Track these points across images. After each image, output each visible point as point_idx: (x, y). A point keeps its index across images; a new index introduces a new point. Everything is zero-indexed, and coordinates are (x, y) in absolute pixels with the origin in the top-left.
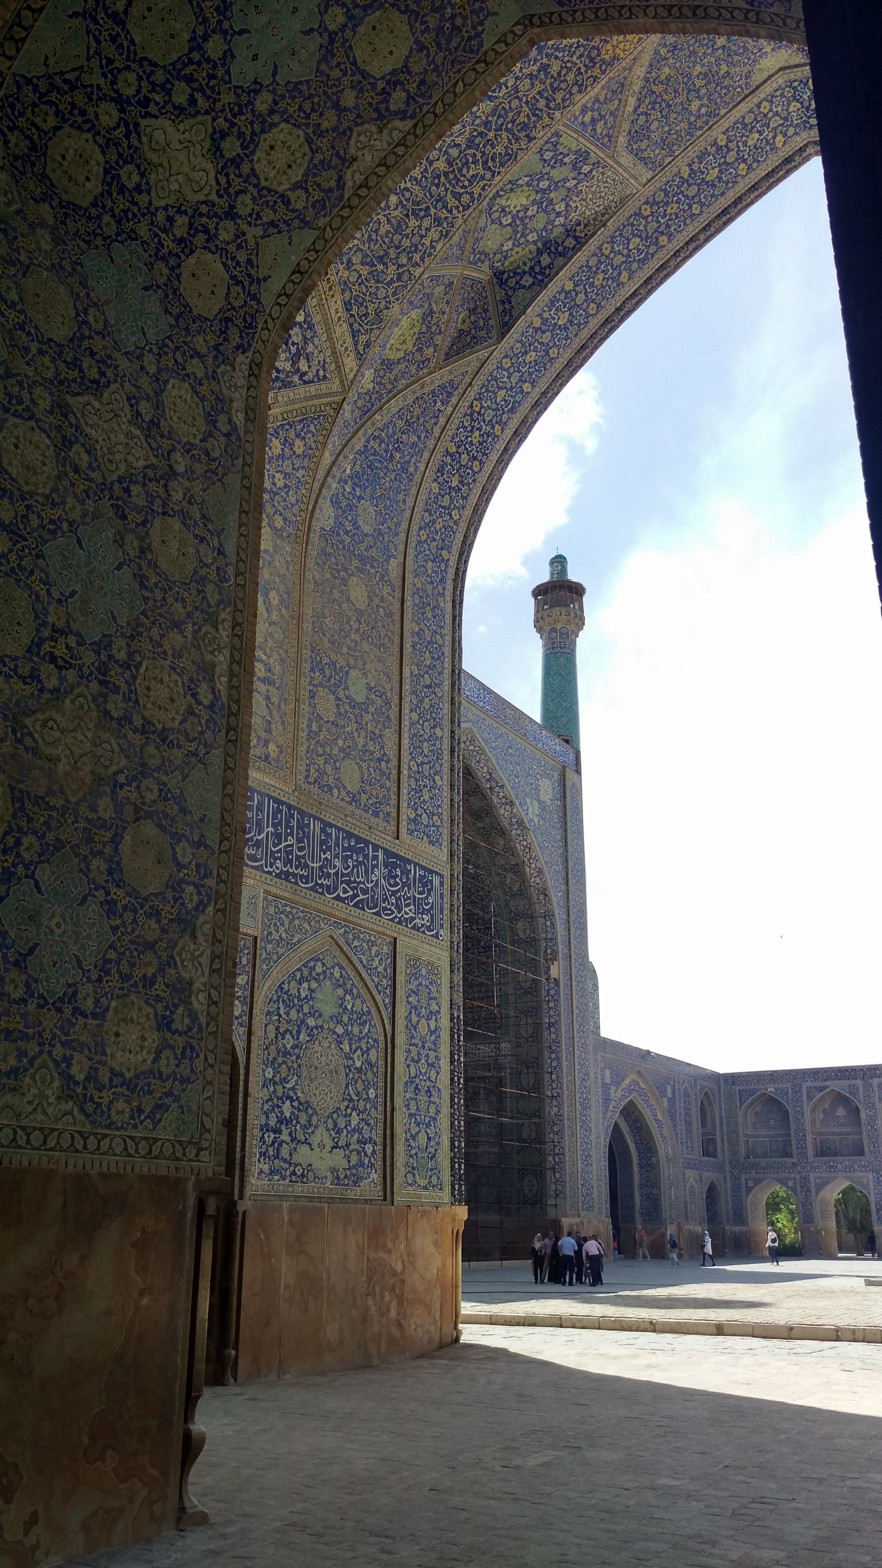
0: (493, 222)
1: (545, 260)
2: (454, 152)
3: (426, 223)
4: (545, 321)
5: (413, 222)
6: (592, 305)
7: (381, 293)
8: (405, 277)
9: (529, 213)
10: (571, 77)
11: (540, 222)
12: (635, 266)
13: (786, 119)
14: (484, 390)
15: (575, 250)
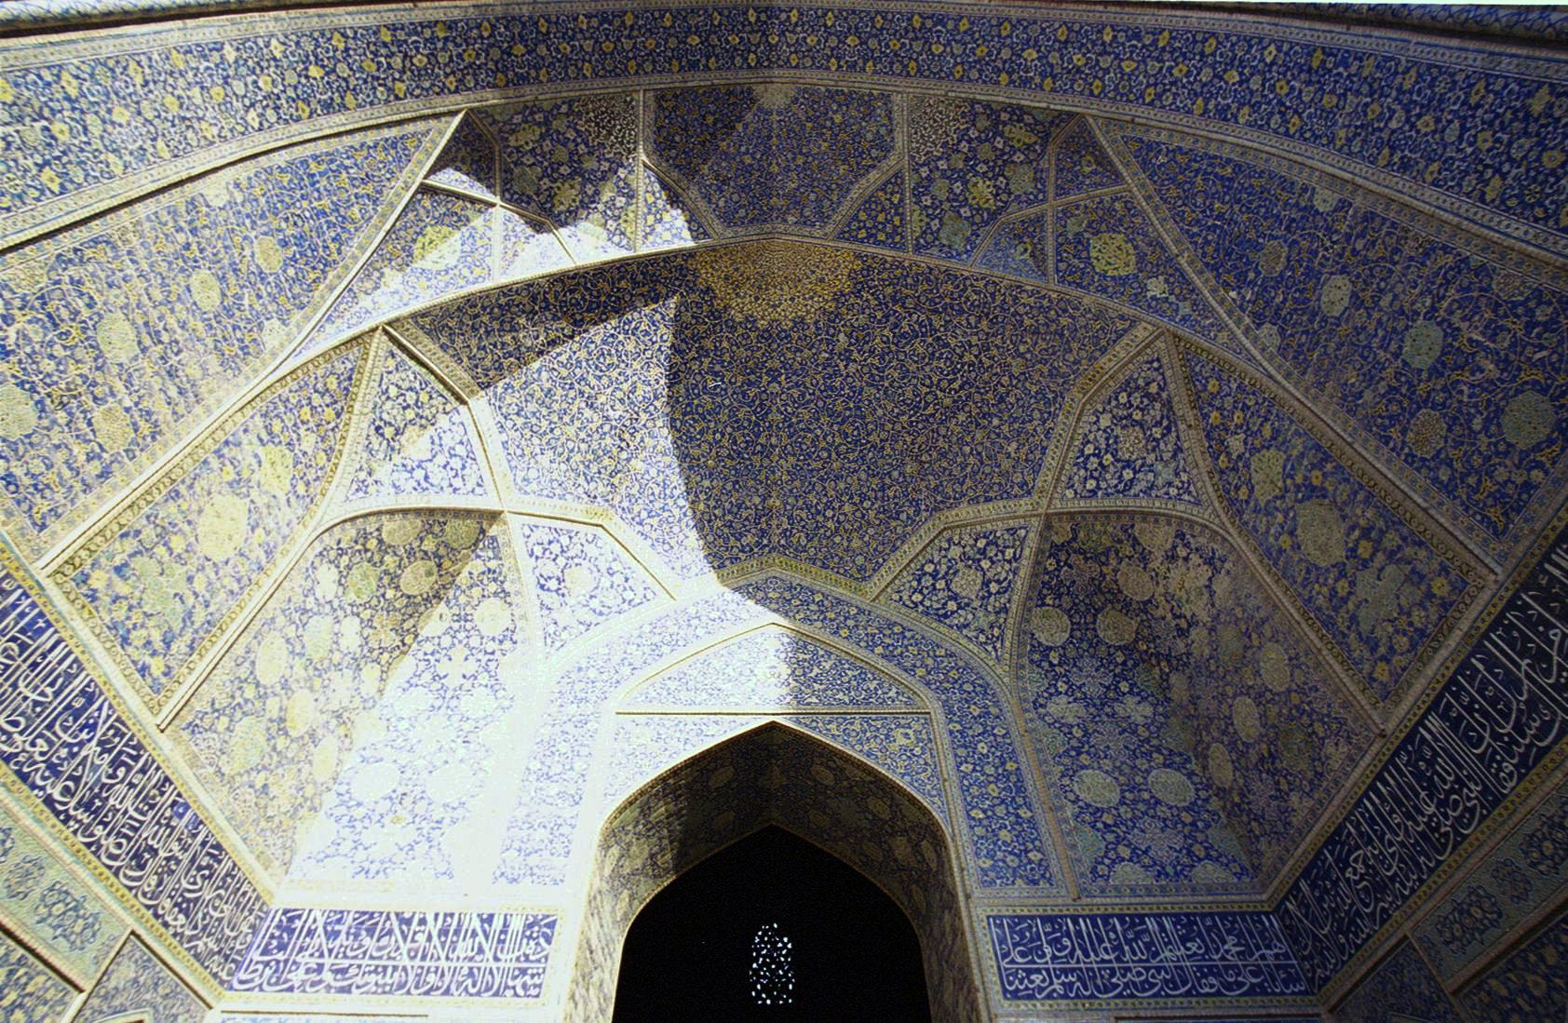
0: (1010, 194)
1: (1004, 117)
2: (972, 320)
3: (1021, 310)
4: (1044, 77)
5: (1027, 322)
6: (1004, 33)
7: (1082, 321)
8: (1062, 305)
9: (985, 168)
10: (885, 276)
11: (985, 151)
12: (950, 25)
13: (783, 33)
14: (1132, 97)
15: (979, 102)
